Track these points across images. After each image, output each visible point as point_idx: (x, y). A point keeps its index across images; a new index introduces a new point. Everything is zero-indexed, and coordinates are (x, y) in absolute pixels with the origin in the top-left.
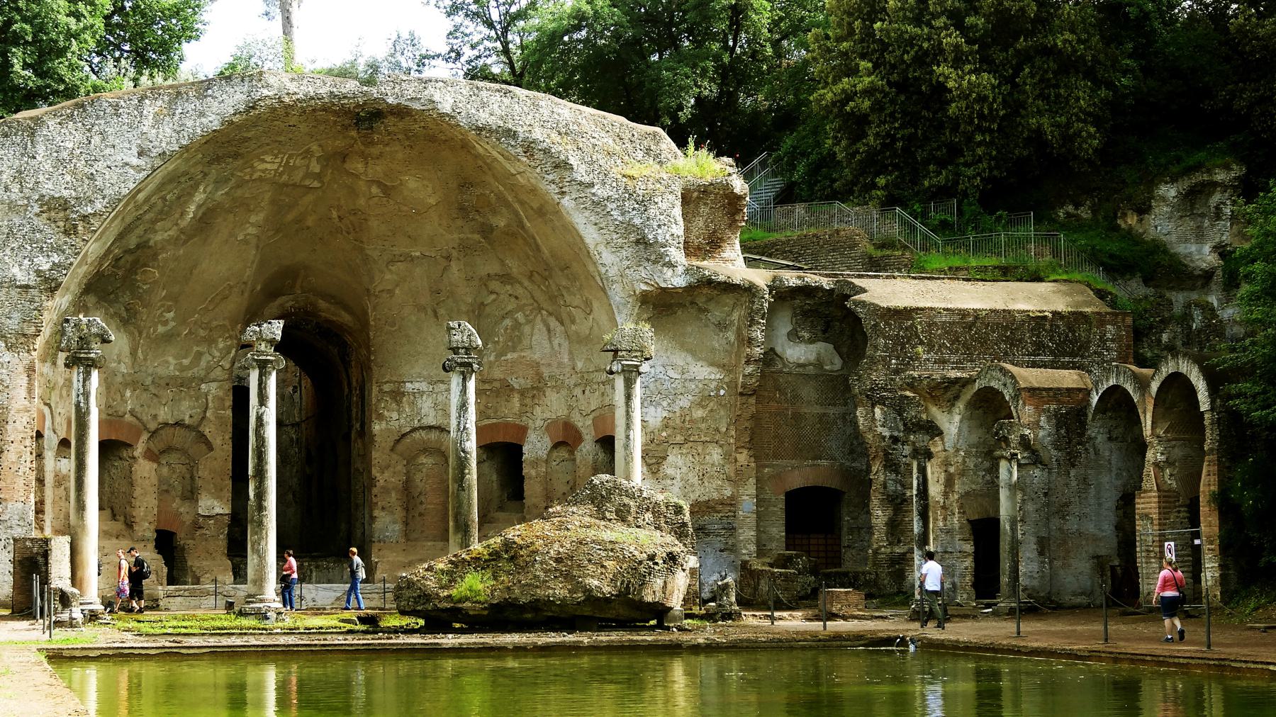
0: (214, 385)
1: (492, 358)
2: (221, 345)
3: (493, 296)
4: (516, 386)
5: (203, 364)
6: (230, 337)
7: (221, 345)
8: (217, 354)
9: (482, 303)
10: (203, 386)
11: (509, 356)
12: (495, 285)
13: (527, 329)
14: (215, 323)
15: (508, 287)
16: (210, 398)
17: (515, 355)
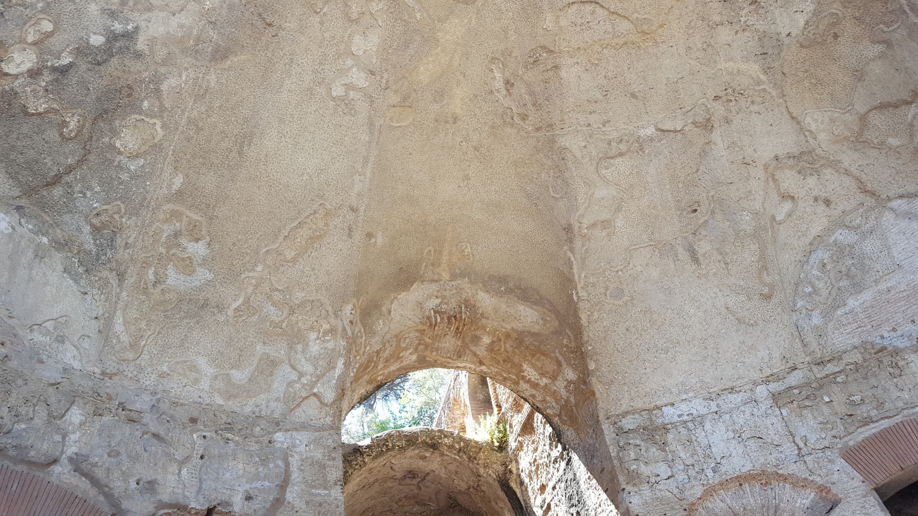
0: (302, 437)
1: (817, 320)
2: (315, 348)
3: (787, 206)
4: (901, 344)
5: (278, 386)
6: (332, 331)
7: (315, 348)
8: (308, 368)
9: (773, 218)
10: (279, 437)
11: (852, 303)
12: (789, 179)
13: (870, 246)
14: (299, 296)
15: (811, 181)
16: (294, 461)
17: (867, 296)
